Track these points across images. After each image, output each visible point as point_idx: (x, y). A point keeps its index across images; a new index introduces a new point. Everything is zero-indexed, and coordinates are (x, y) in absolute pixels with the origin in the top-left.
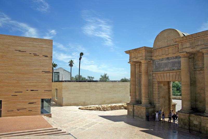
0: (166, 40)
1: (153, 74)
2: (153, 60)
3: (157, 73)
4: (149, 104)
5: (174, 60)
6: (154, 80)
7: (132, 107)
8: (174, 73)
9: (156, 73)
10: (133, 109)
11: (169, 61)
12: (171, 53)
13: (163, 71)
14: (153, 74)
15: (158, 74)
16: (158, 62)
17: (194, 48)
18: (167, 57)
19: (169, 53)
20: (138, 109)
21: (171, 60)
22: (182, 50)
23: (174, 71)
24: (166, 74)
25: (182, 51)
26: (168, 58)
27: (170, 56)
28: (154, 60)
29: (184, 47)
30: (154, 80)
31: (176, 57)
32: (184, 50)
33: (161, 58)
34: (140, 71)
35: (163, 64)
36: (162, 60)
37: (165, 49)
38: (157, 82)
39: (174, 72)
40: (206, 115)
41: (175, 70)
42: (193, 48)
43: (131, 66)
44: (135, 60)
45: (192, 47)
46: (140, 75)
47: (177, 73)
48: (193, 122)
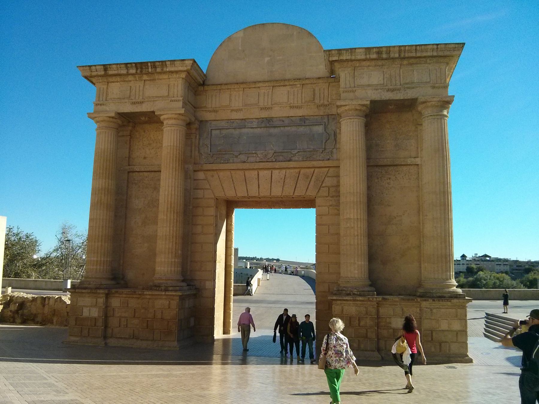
0: (267, 59)
1: (195, 171)
2: (202, 121)
3: (214, 167)
4: (183, 281)
5: (294, 129)
6: (200, 193)
7: (101, 301)
8: (292, 171)
9: (214, 168)
10: (107, 306)
11: (272, 130)
12: (284, 103)
13: (244, 162)
14: (195, 171)
15: (221, 174)
16: (224, 132)
17: (399, 90)
18: (265, 114)
19: (276, 104)
20: (133, 303)
21: (282, 128)
22: (354, 92)
23: (291, 164)
24: (256, 172)
25: (351, 95)
26: (269, 120)
27: (277, 113)
28: (207, 121)
29: (364, 81)
30: (200, 193)
31: (303, 121)
32: (360, 93)
33: (235, 116)
34: (129, 157)
35: (245, 137)
36: (243, 123)
37: (259, 87)
38: (212, 203)
39: (292, 166)
40: (438, 295)
41: (295, 161)
42: (393, 90)
43: (97, 130)
44: (127, 108)
45: (391, 87)
46: (129, 172)
47: (303, 171)
48: (390, 323)
